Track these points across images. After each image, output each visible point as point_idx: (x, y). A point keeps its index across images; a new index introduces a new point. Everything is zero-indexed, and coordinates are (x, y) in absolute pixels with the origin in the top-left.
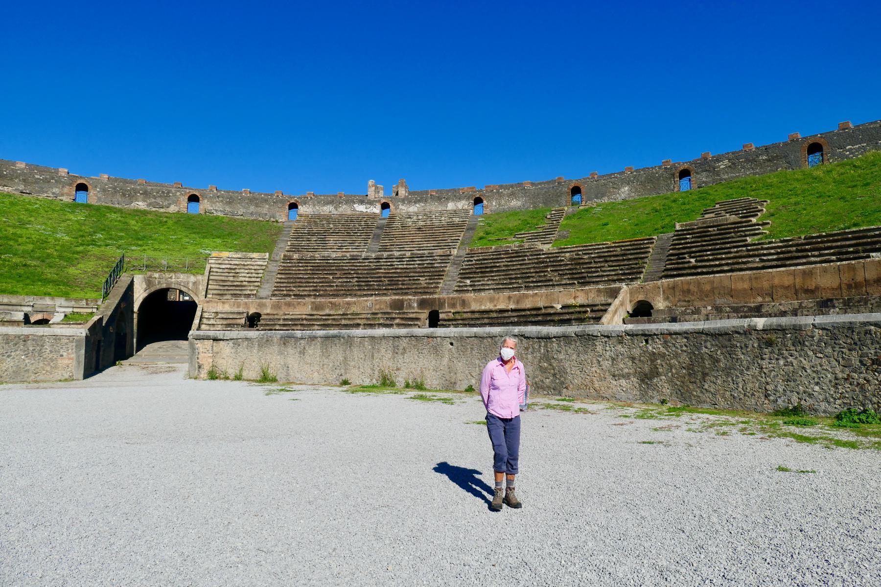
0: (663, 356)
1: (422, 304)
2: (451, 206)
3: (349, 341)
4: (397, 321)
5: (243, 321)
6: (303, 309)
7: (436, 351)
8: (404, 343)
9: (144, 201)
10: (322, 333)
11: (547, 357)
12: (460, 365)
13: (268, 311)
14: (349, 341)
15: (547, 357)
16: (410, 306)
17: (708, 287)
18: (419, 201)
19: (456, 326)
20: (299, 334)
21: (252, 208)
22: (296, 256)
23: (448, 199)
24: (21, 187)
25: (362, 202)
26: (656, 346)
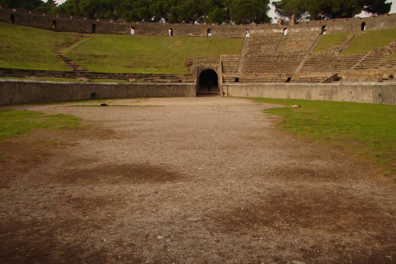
0: (327, 90)
1: (287, 75)
2: (312, 29)
3: (264, 86)
4: (279, 81)
5: (234, 80)
6: (250, 77)
7: (285, 89)
8: (278, 87)
9: (192, 33)
10: (257, 84)
11: (308, 91)
12: (291, 92)
13: (241, 77)
14: (264, 86)
15: (308, 91)
16: (283, 76)
17: (353, 74)
18: (300, 27)
19: (294, 82)
20: (250, 84)
21: (232, 33)
22: (249, 56)
23: (311, 26)
24: (153, 32)
25: (275, 28)
26: (326, 88)
